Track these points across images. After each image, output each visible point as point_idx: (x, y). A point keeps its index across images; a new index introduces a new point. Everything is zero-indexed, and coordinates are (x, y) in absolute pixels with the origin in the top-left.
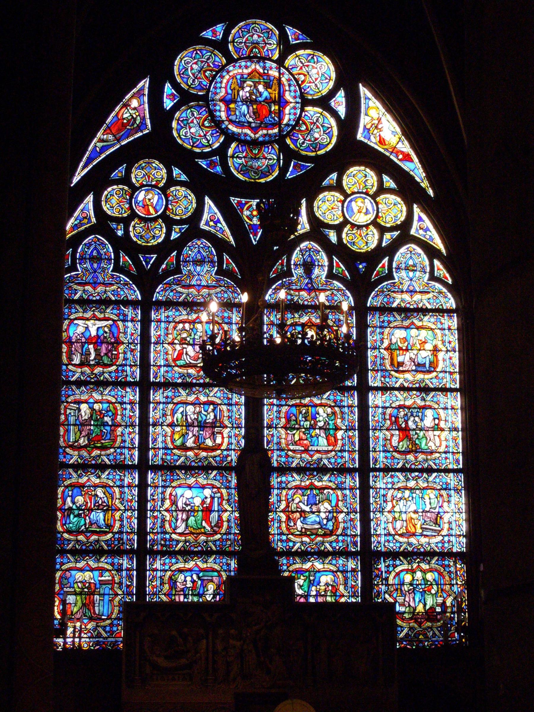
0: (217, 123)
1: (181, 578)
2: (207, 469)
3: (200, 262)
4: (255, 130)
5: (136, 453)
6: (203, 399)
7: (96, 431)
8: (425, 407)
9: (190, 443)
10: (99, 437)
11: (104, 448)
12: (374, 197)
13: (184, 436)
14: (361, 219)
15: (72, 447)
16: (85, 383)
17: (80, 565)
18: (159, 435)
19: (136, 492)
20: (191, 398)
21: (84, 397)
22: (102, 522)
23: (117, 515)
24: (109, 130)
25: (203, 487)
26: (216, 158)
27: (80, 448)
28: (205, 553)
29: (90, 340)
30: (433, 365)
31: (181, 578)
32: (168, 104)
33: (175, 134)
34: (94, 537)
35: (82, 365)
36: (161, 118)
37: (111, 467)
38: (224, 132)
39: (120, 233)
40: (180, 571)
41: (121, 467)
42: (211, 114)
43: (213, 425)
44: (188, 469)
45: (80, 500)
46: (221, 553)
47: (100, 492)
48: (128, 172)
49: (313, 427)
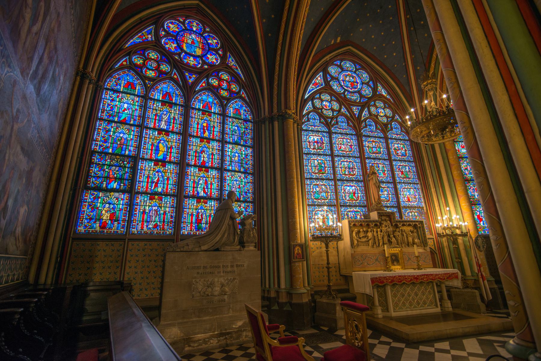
0: (342, 86)
1: (350, 214)
2: (352, 181)
3: (343, 122)
4: (351, 89)
6: (349, 160)
7: (320, 169)
8: (406, 166)
9: (347, 173)
10: (321, 170)
11: (323, 174)
12: (383, 109)
13: (345, 171)
14: (382, 114)
16: (316, 154)
17: (320, 209)
18: (338, 170)
20: (345, 160)
21: (316, 158)
23: (329, 194)
24: (313, 84)
25: (352, 186)
27: (316, 173)
28: (355, 206)
29: (315, 142)
30: (406, 154)
31: (350, 214)
34: (323, 201)
35: (314, 149)
36: (327, 83)
40: (350, 211)
41: (329, 179)
43: (352, 168)
44: (347, 181)
45: (318, 189)
46: (360, 206)
47: (323, 187)
49: (379, 170)
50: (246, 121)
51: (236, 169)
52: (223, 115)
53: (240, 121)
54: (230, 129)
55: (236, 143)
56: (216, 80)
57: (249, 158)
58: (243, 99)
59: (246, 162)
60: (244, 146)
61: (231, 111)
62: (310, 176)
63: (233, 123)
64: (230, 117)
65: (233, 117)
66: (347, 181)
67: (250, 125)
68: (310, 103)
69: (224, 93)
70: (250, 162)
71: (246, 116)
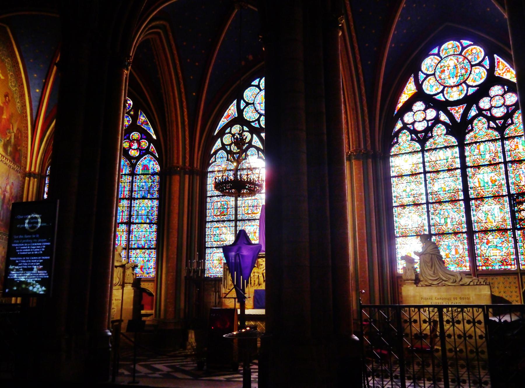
0: (257, 111)
5: (234, 216)
7: (222, 210)
9: (250, 212)
10: (223, 212)
11: (225, 215)
15: (215, 215)
17: (218, 251)
19: (234, 228)
21: (219, 200)
22: (224, 238)
26: (257, 122)
32: (242, 107)
33: (244, 116)
34: (222, 243)
36: (240, 112)
37: (227, 221)
38: (259, 113)
39: (228, 149)
41: (229, 221)
42: (255, 108)
44: (249, 220)
48: (231, 130)
50: (154, 174)
51: (143, 222)
52: (133, 174)
53: (148, 176)
54: (138, 186)
55: (144, 198)
56: (127, 142)
57: (155, 209)
58: (152, 154)
59: (152, 214)
60: (150, 199)
61: (139, 169)
62: (212, 219)
63: (141, 179)
64: (138, 175)
65: (141, 174)
66: (249, 220)
67: (157, 177)
68: (219, 140)
69: (134, 153)
70: (156, 213)
71: (154, 169)
